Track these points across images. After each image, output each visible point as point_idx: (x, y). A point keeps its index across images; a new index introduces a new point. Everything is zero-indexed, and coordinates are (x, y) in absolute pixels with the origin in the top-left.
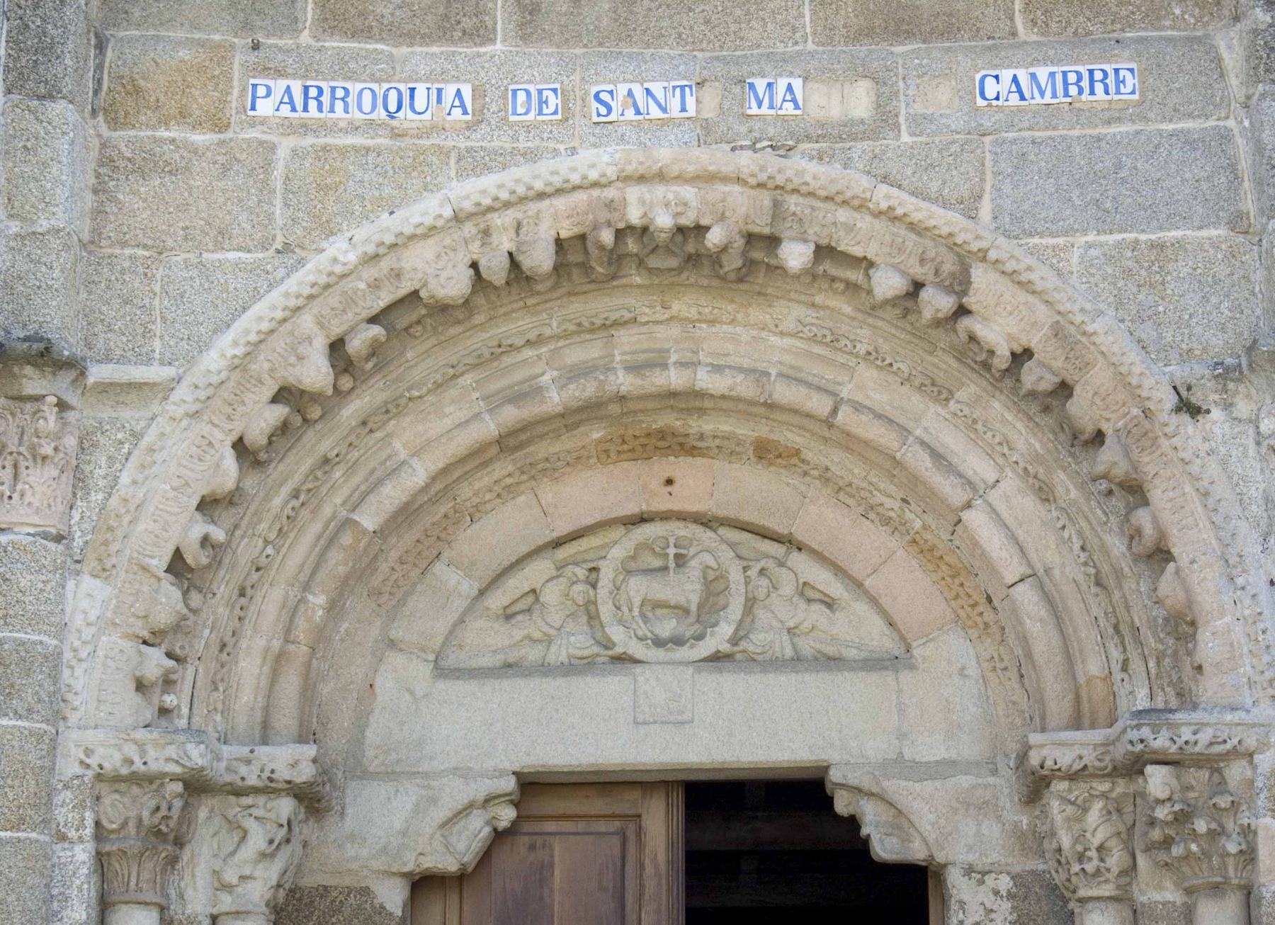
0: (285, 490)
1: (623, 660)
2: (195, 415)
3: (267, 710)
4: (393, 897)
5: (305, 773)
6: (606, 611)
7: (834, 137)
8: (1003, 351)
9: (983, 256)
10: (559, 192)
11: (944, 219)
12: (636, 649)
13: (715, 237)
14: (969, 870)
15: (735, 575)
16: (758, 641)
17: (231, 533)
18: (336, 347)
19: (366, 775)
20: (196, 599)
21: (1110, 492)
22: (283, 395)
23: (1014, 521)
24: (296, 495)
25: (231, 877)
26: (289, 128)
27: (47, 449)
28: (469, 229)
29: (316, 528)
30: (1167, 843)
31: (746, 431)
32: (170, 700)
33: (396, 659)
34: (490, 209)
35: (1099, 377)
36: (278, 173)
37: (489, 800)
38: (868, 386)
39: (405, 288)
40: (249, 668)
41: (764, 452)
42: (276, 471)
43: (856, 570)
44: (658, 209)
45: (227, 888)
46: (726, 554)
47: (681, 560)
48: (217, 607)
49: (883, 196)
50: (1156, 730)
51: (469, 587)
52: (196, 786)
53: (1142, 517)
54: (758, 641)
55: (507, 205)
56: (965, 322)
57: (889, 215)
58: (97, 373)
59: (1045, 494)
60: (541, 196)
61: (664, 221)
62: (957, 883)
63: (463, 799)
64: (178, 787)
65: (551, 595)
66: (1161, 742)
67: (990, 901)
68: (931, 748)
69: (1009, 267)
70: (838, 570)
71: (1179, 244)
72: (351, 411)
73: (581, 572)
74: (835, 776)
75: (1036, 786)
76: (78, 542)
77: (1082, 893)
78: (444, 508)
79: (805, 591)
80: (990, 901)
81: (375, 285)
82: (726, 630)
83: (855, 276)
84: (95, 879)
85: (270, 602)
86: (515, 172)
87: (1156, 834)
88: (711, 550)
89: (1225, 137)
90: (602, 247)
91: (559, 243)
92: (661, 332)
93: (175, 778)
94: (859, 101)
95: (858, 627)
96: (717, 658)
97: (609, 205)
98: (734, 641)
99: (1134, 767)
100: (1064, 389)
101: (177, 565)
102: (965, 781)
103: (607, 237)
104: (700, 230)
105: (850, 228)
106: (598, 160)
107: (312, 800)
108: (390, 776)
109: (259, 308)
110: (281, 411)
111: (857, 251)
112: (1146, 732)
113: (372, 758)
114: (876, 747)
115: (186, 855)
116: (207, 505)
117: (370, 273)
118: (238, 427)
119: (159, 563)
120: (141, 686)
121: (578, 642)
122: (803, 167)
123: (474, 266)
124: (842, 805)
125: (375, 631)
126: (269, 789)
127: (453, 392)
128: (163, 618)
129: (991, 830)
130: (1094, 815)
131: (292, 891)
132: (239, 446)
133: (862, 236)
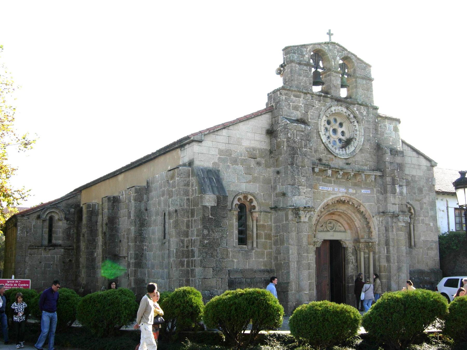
7: (353, 194)
16: (337, 229)
23: (358, 223)
26: (322, 190)
31: (338, 213)
35: (368, 214)
38: (349, 212)
41: (339, 215)
44: (343, 199)
49: (357, 199)
54: (337, 229)
59: (360, 221)
62: (349, 249)
68: (348, 239)
70: (342, 225)
79: (340, 226)
94: (354, 192)
95: (342, 229)
99: (369, 243)
106: (340, 195)
114: (344, 238)
121: (325, 229)
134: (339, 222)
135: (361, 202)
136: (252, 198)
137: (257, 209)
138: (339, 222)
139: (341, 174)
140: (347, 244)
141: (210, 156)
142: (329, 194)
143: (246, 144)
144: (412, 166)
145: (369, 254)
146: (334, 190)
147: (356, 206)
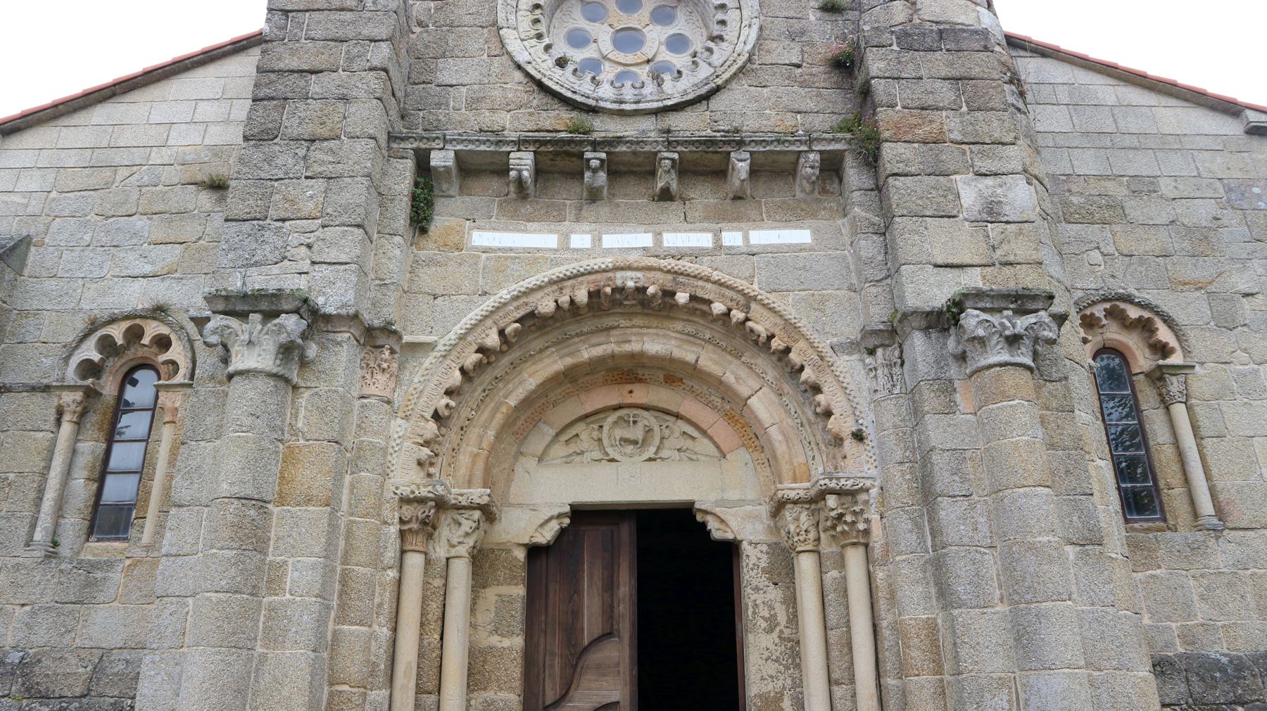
0: (480, 389)
1: (612, 460)
2: (444, 357)
3: (471, 476)
4: (521, 555)
5: (485, 500)
6: (606, 442)
8: (764, 335)
9: (754, 298)
10: (590, 273)
11: (741, 284)
12: (617, 457)
13: (651, 290)
14: (750, 543)
15: (656, 429)
17: (457, 406)
18: (501, 333)
19: (510, 505)
20: (443, 430)
21: (806, 391)
22: (481, 350)
24: (484, 391)
25: (455, 541)
27: (385, 365)
28: (555, 287)
29: (492, 405)
30: (834, 527)
32: (432, 470)
33: (522, 459)
34: (563, 280)
36: (481, 265)
37: (559, 516)
39: (529, 309)
40: (464, 459)
42: (477, 382)
43: (704, 426)
44: (630, 280)
45: (453, 546)
46: (653, 420)
47: (635, 422)
48: (453, 436)
49: (716, 275)
50: (831, 479)
51: (552, 432)
52: (441, 504)
53: (820, 398)
55: (570, 278)
56: (749, 324)
57: (718, 283)
58: (407, 338)
60: (583, 274)
61: (630, 284)
63: (549, 515)
64: (433, 503)
65: (584, 436)
66: (833, 484)
67: (759, 555)
68: (733, 495)
69: (766, 301)
71: (830, 295)
72: (505, 361)
73: (596, 426)
74: (697, 506)
75: (779, 507)
76: (396, 405)
77: (799, 549)
78: (543, 401)
80: (759, 555)
81: (517, 308)
82: (653, 449)
83: (704, 307)
84: (398, 540)
85: (474, 433)
86: (573, 265)
87: (829, 523)
88: (648, 418)
89: (845, 257)
90: (606, 294)
91: (589, 293)
92: (629, 331)
93: (431, 500)
96: (650, 460)
97: (610, 279)
98: (656, 453)
99: (822, 495)
100: (788, 350)
101: (436, 416)
102: (749, 508)
103: (608, 290)
104: (645, 289)
105: (703, 288)
107: (488, 513)
108: (520, 505)
109: (471, 315)
110: (479, 355)
111: (706, 297)
112: (827, 481)
113: (512, 499)
115: (436, 534)
116: (449, 393)
117: (515, 304)
118: (461, 361)
119: (428, 415)
120: (420, 464)
122: (685, 265)
123: (556, 301)
124: (699, 518)
125: (514, 449)
126: (471, 507)
127: (548, 352)
128: (428, 435)
129: (759, 527)
130: (803, 517)
131: (480, 551)
132: (462, 370)
133: (707, 291)
134: (678, 416)
135: (754, 289)
136: (165, 330)
137: (179, 378)
138: (678, 416)
139: (595, 163)
140: (733, 523)
141: (17, 198)
142: (532, 257)
143: (186, 140)
144: (1128, 141)
145: (841, 564)
146: (565, 246)
147: (718, 308)
